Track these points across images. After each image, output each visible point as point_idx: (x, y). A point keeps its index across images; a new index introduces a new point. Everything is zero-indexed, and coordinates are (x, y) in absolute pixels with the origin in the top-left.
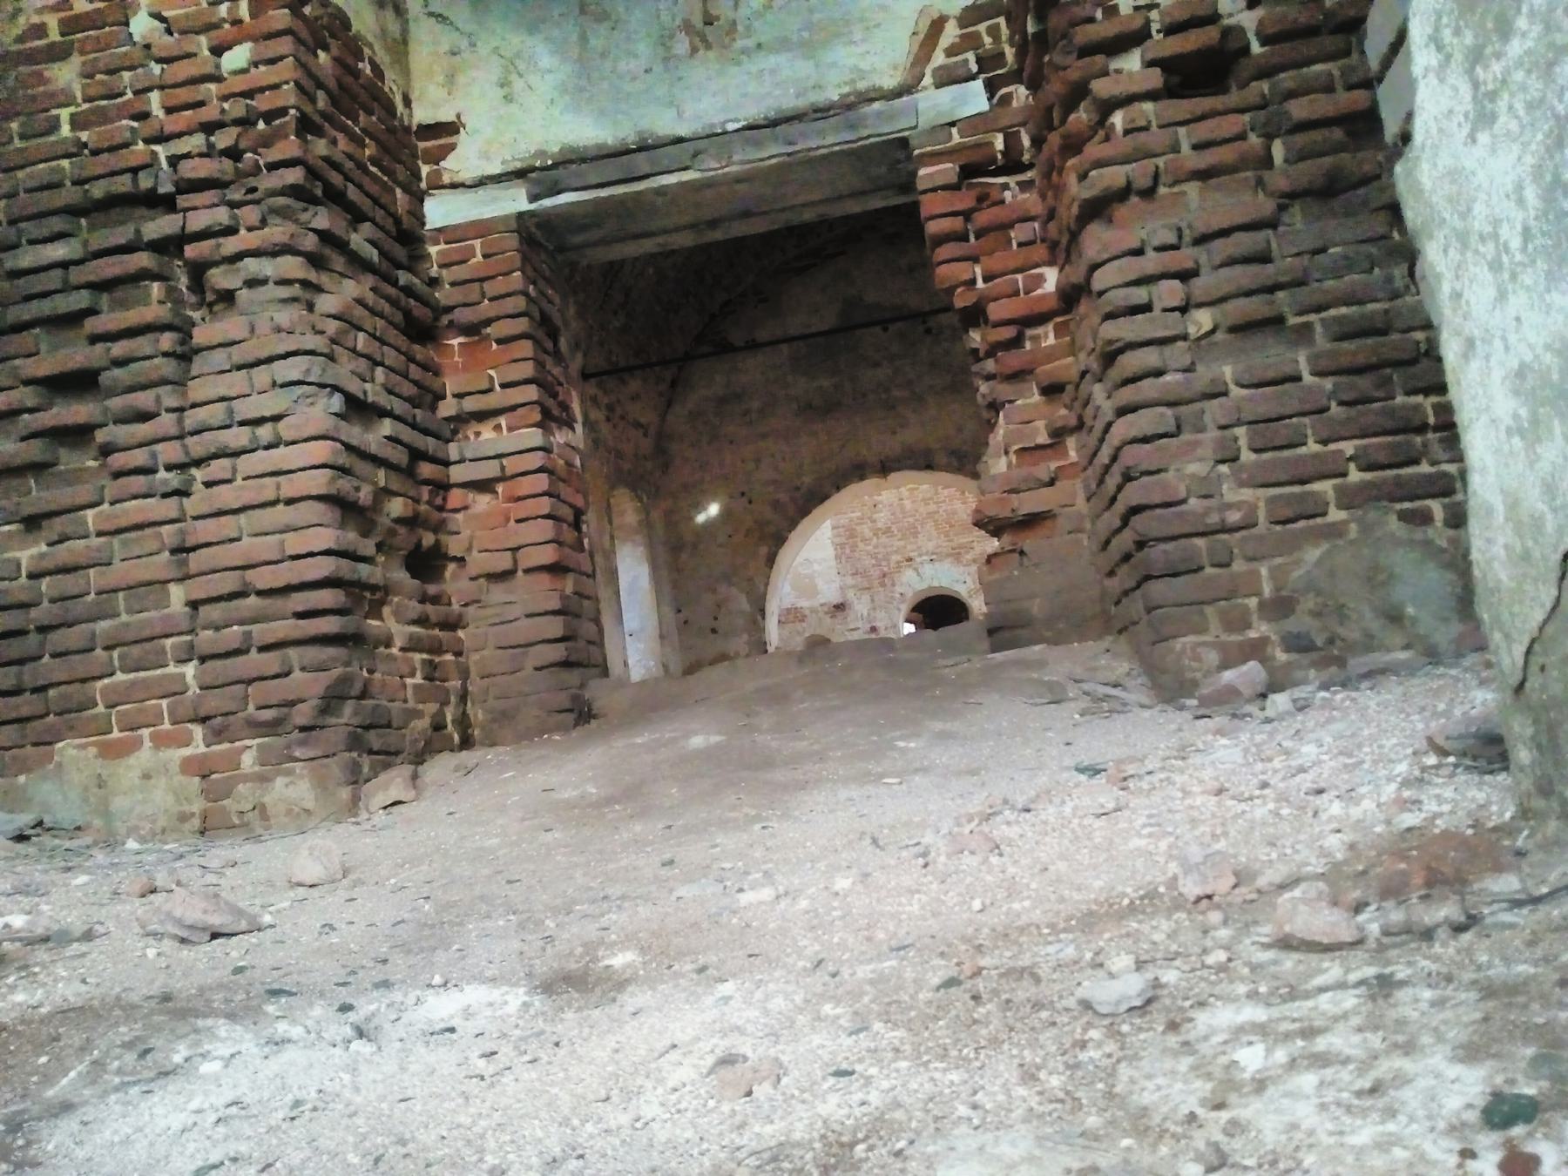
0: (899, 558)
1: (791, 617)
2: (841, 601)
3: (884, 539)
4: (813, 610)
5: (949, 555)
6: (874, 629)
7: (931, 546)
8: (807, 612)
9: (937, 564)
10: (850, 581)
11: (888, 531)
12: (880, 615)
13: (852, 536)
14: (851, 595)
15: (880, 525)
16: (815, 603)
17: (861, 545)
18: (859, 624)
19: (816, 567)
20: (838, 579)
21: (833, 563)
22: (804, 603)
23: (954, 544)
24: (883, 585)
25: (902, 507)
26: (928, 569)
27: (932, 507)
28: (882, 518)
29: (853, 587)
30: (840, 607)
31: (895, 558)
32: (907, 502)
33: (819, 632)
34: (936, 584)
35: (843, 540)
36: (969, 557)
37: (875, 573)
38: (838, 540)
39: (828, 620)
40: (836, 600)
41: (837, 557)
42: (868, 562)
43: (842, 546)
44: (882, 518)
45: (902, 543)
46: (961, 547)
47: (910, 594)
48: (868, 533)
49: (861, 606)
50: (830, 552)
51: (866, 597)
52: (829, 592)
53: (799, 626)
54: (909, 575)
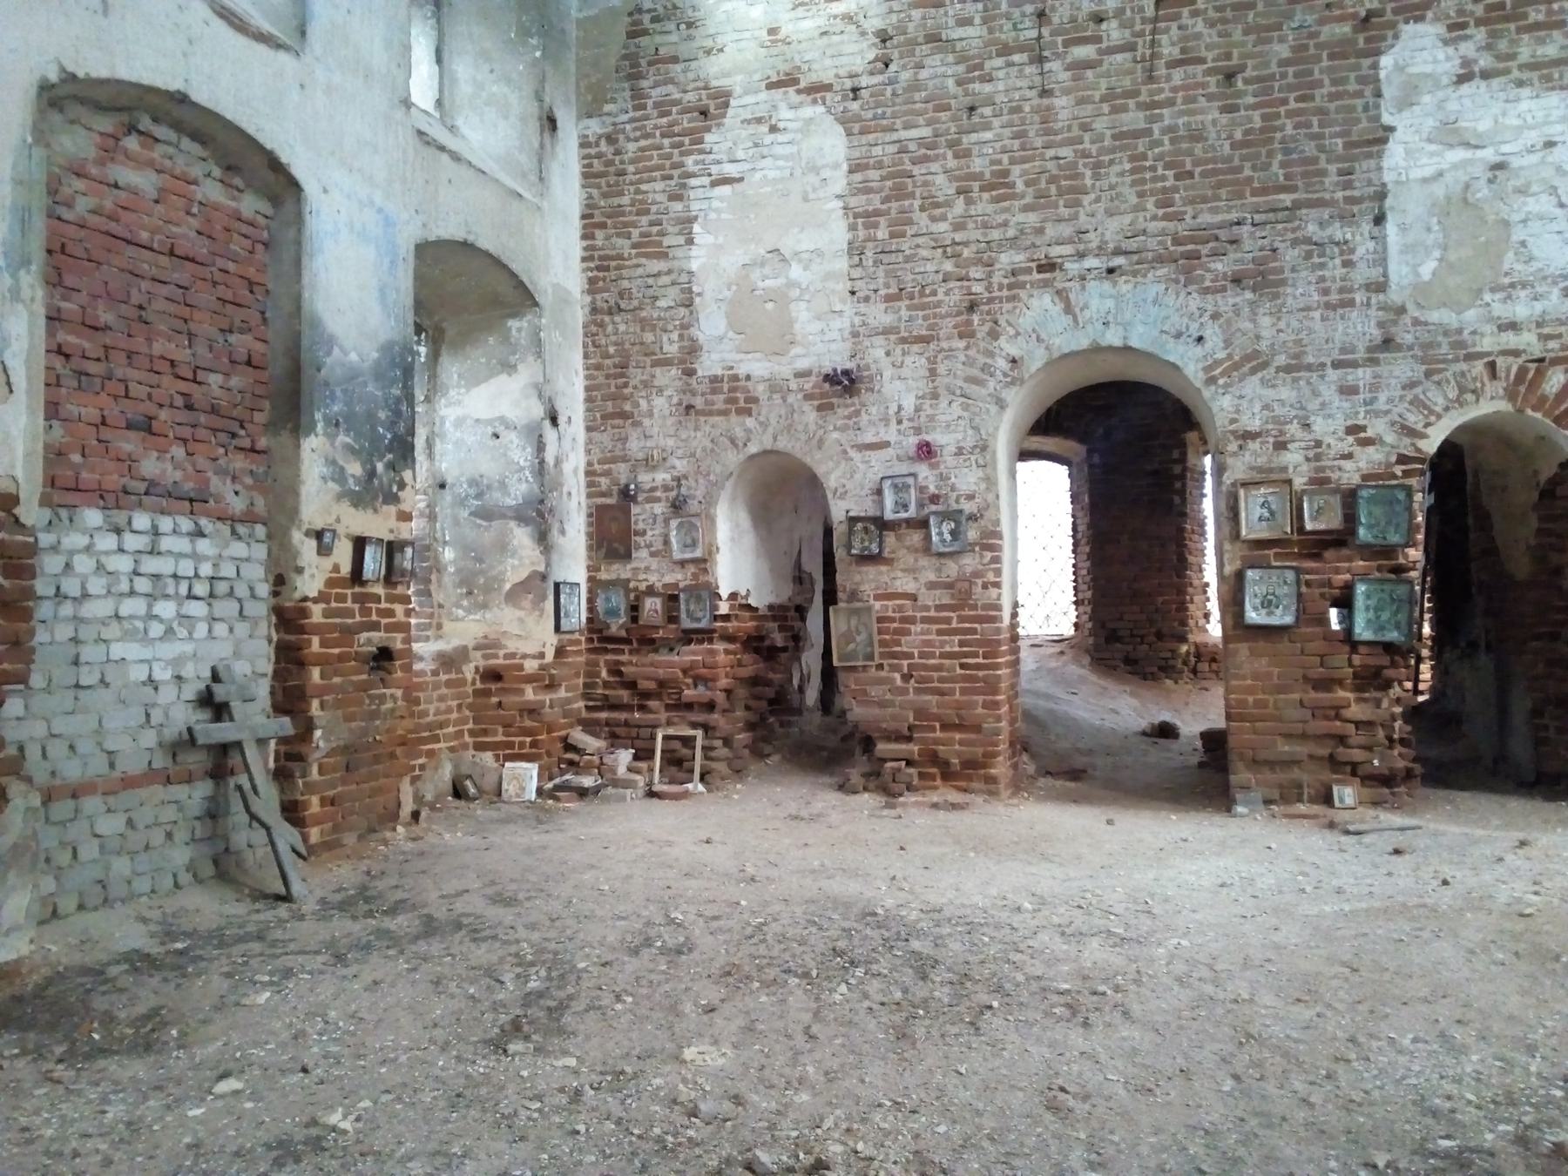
0: (1019, 258)
1: (719, 401)
2: (843, 363)
3: (984, 205)
4: (776, 387)
5: (1160, 260)
6: (926, 451)
7: (1113, 229)
8: (760, 390)
9: (1124, 285)
10: (879, 315)
11: (999, 184)
12: (949, 411)
13: (900, 193)
14: (876, 352)
15: (978, 164)
16: (783, 368)
17: (922, 219)
18: (891, 434)
19: (796, 271)
20: (848, 308)
21: (842, 264)
22: (756, 367)
23: (1181, 229)
24: (966, 333)
25: (1046, 116)
26: (1097, 298)
27: (1133, 118)
28: (988, 145)
29: (886, 332)
30: (844, 384)
31: (1006, 259)
32: (1060, 102)
33: (783, 444)
34: (1113, 338)
35: (876, 202)
36: (1219, 266)
37: (950, 297)
38: (856, 202)
39: (811, 416)
40: (836, 357)
41: (855, 250)
42: (934, 265)
43: (871, 217)
44: (988, 145)
45: (1032, 218)
46: (1204, 235)
47: (1036, 361)
48: (943, 186)
49: (899, 385)
50: (838, 233)
51: (915, 363)
52: (822, 341)
53: (738, 425)
54: (1040, 307)
